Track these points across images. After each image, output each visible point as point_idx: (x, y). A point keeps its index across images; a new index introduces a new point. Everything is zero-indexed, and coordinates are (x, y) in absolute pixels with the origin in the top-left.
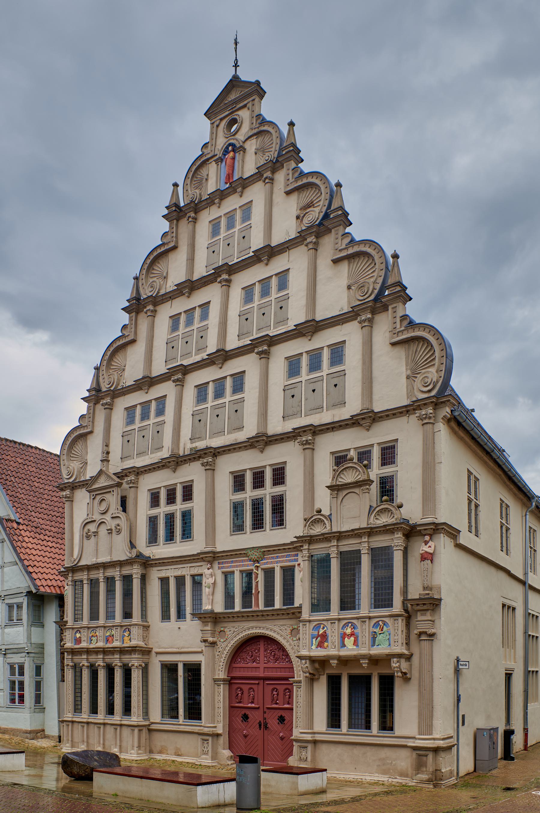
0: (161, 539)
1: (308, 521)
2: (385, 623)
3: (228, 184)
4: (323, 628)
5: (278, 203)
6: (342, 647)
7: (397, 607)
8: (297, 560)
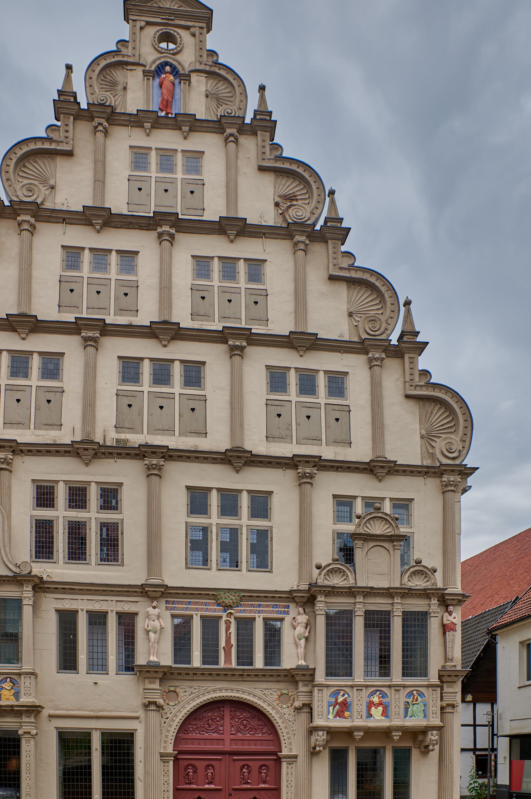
0: (61, 555)
1: (324, 569)
2: (421, 694)
3: (164, 112)
4: (343, 695)
5: (245, 173)
6: (367, 717)
7: (434, 678)
8: (288, 613)
